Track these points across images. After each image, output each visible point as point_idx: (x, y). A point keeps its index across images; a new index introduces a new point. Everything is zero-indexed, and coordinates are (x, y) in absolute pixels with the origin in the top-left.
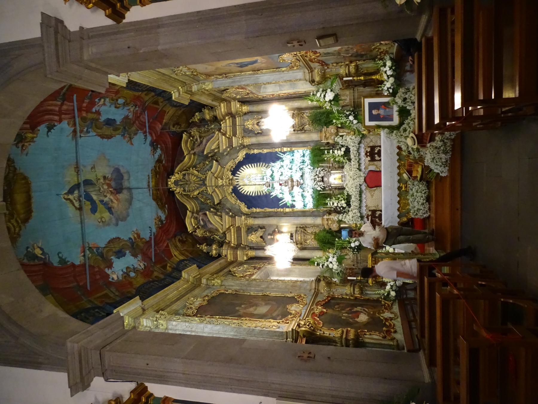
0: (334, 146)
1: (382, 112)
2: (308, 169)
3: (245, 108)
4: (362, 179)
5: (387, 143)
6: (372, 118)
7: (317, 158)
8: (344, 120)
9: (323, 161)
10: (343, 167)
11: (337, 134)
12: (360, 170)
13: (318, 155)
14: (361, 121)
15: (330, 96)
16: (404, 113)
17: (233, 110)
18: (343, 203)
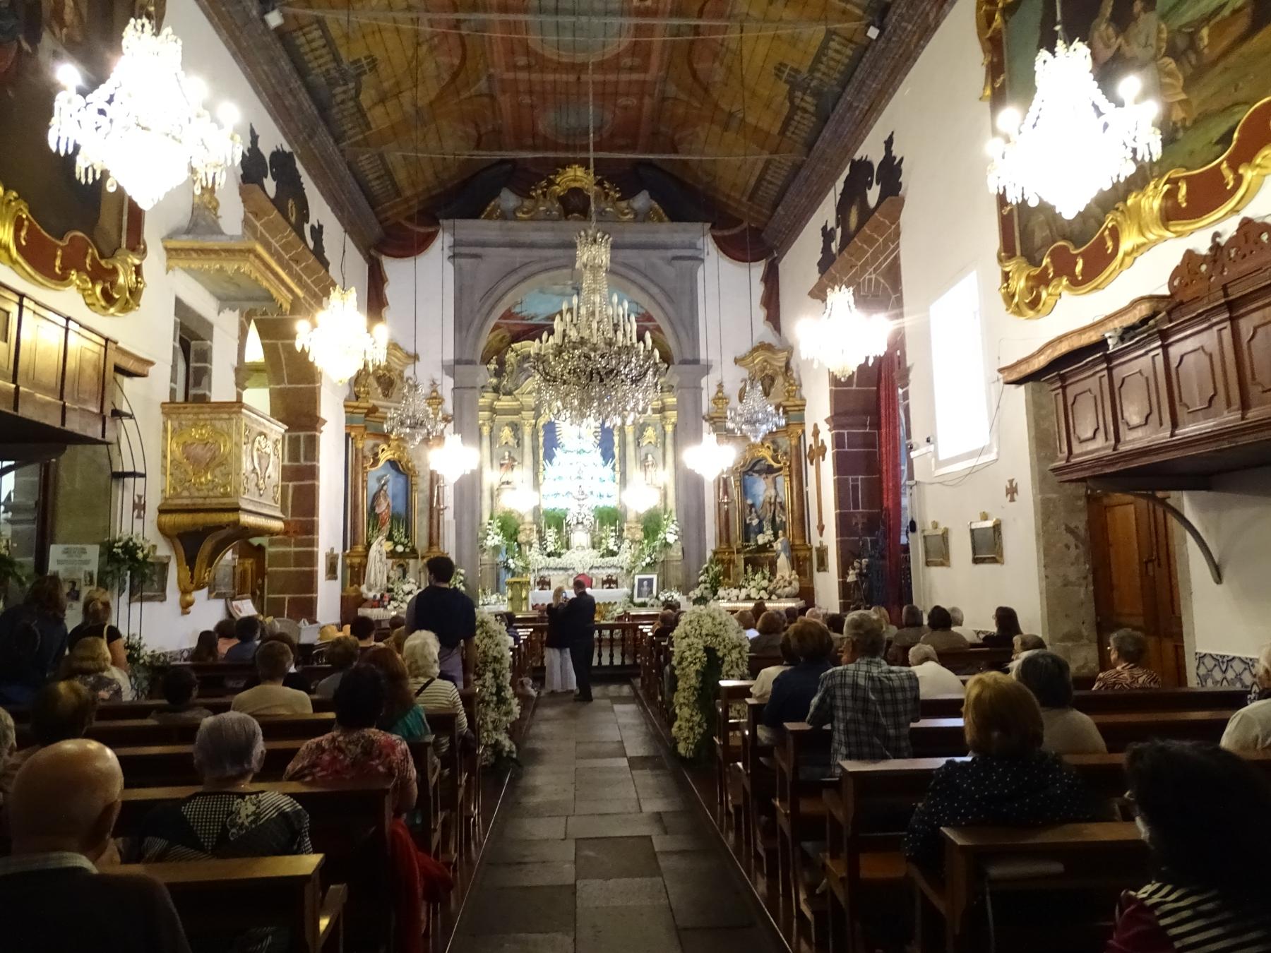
0: (620, 537)
1: (645, 588)
2: (593, 502)
3: (669, 428)
4: (581, 571)
5: (618, 595)
6: (641, 581)
7: (605, 516)
8: (647, 552)
9: (602, 524)
10: (594, 547)
11: (633, 541)
12: (591, 568)
13: (610, 518)
14: (644, 571)
15: (671, 539)
16: (644, 605)
17: (668, 413)
18: (551, 548)
